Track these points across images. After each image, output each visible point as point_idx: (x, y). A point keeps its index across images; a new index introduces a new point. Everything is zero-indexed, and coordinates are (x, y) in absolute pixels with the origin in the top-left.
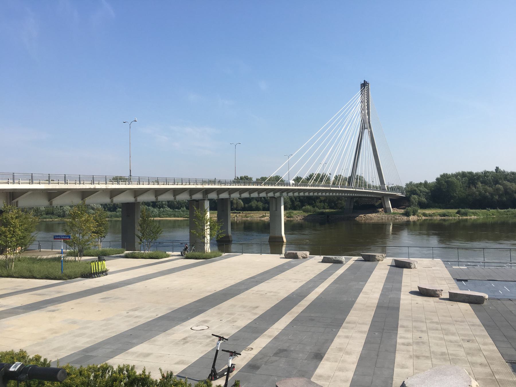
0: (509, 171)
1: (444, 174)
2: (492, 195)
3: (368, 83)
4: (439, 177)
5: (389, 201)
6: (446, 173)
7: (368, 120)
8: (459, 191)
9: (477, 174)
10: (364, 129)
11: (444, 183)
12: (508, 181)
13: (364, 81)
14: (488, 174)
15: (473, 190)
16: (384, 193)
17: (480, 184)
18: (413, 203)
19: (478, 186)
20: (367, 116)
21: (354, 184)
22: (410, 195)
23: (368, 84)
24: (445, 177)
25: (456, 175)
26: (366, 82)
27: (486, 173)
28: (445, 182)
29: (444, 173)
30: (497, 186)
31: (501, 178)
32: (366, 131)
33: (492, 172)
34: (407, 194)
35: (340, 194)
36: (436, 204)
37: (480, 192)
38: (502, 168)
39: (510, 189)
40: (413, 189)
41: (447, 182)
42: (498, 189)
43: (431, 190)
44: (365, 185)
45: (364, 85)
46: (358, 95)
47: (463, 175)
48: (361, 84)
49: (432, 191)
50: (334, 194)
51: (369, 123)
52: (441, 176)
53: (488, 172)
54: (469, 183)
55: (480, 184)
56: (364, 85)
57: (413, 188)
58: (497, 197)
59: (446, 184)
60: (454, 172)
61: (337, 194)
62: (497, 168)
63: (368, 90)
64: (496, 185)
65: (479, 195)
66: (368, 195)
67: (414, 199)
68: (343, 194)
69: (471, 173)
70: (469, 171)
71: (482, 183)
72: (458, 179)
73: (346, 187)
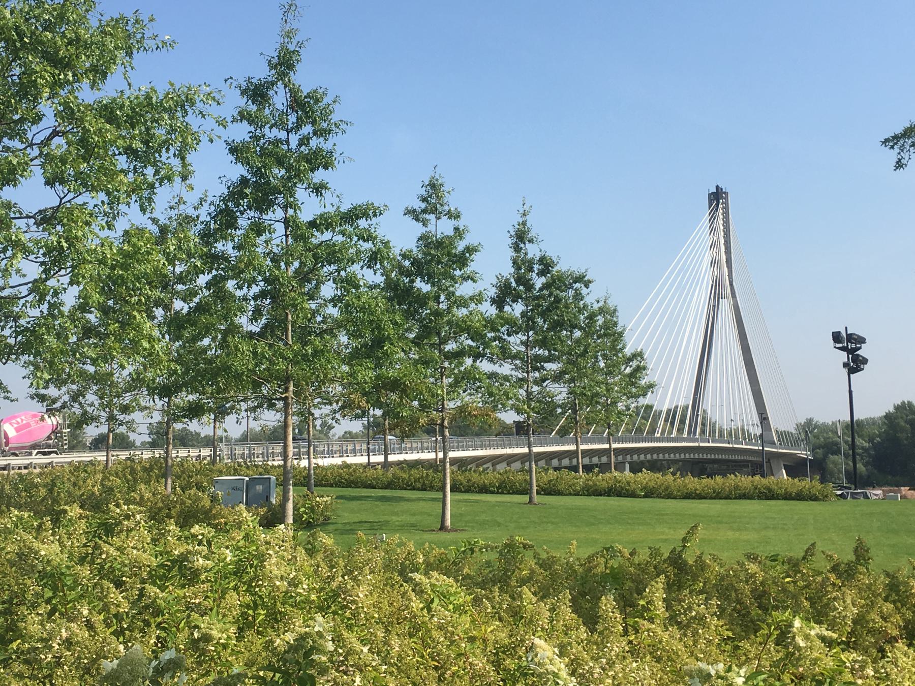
3: (725, 193)
4: (892, 410)
5: (784, 471)
6: (908, 402)
7: (727, 277)
10: (719, 298)
11: (903, 424)
13: (717, 187)
16: (776, 450)
18: (832, 475)
22: (825, 456)
26: (720, 190)
29: (904, 402)
32: (725, 306)
34: (817, 453)
35: (655, 456)
40: (830, 440)
44: (721, 435)
45: (717, 197)
46: (706, 220)
48: (710, 195)
49: (875, 447)
50: (642, 457)
52: (897, 408)
56: (717, 197)
57: (828, 438)
59: (908, 426)
61: (649, 457)
66: (692, 455)
68: (661, 456)
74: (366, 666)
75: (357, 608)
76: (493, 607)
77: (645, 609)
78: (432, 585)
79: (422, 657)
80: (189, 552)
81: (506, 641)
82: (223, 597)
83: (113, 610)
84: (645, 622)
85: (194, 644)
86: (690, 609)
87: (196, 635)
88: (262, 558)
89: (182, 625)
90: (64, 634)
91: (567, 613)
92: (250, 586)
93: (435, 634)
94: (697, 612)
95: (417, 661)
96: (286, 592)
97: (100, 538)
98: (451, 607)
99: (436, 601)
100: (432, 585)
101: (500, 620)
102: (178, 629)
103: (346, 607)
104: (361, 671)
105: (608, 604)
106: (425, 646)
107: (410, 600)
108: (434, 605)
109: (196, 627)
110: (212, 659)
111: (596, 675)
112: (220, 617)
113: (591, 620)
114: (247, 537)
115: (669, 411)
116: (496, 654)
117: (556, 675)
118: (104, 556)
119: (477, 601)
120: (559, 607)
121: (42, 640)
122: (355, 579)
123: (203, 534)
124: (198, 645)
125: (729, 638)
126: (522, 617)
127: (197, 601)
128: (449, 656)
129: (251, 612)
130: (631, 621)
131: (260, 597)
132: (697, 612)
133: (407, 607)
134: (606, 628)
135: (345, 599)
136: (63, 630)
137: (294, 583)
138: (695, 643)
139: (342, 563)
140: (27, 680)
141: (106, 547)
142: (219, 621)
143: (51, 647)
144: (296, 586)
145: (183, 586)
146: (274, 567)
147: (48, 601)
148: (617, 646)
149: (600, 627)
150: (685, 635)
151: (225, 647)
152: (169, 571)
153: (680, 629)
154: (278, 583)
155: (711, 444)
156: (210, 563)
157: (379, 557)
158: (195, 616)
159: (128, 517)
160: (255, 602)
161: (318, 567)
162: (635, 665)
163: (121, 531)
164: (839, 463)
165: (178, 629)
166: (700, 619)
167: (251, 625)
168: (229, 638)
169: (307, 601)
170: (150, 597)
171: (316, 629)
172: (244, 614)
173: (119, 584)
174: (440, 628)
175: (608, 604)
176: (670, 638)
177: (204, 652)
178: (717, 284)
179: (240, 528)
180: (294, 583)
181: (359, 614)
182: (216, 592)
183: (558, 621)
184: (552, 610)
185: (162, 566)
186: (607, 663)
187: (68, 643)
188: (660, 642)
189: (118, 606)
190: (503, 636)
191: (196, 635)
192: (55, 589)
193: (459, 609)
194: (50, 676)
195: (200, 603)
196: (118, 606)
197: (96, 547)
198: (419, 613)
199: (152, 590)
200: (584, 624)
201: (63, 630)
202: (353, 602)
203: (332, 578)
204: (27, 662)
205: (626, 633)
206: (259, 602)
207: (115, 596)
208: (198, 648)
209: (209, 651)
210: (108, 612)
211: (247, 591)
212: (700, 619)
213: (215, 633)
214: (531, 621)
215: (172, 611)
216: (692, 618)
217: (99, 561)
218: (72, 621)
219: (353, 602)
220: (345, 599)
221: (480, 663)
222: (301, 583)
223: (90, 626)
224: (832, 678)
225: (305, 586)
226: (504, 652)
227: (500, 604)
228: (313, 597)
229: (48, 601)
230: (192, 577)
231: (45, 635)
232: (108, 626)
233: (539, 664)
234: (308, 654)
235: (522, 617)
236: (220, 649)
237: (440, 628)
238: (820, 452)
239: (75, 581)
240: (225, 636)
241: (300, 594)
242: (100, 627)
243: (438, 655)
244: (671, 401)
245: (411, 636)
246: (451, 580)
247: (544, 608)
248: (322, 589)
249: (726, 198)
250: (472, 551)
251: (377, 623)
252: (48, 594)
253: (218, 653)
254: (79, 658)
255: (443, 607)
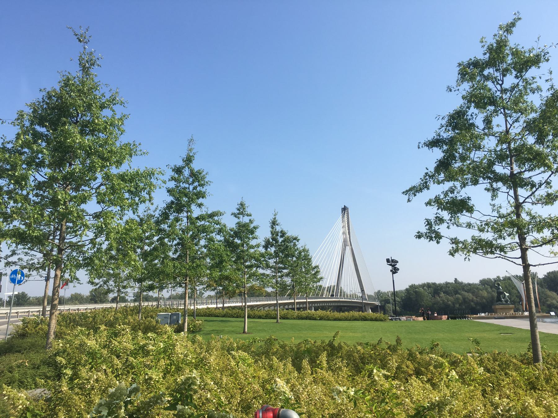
0: (466, 283)
1: (412, 285)
2: (453, 303)
4: (408, 287)
8: (426, 300)
9: (440, 284)
12: (466, 291)
14: (449, 285)
15: (437, 299)
17: (442, 294)
18: (388, 311)
19: (441, 295)
20: (348, 236)
21: (337, 295)
23: (348, 208)
24: (412, 287)
25: (423, 286)
27: (447, 284)
28: (413, 291)
30: (457, 295)
31: (460, 289)
32: (348, 249)
33: (452, 283)
35: (323, 304)
36: (408, 312)
37: (443, 301)
38: (460, 280)
39: (468, 298)
41: (416, 292)
42: (458, 299)
43: (402, 299)
45: (345, 209)
47: (428, 285)
48: (342, 209)
49: (403, 300)
51: (350, 241)
52: (410, 286)
53: (449, 283)
54: (434, 292)
55: (442, 294)
56: (345, 209)
58: (457, 306)
60: (420, 283)
61: (321, 304)
62: (456, 279)
63: (348, 214)
64: (456, 294)
65: (443, 303)
67: (389, 307)
69: (434, 284)
70: (433, 282)
71: (444, 293)
72: (425, 290)
73: (328, 298)
74: (212, 390)
75: (210, 365)
76: (262, 364)
77: (319, 364)
78: (239, 356)
79: (235, 384)
80: (147, 344)
81: (267, 378)
82: (158, 361)
83: (115, 367)
84: (319, 370)
85: (146, 381)
86: (336, 364)
87: (146, 377)
88: (174, 346)
89: (142, 372)
90: (95, 377)
91: (290, 366)
92: (169, 357)
93: (240, 375)
94: (339, 366)
95: (233, 386)
96: (183, 359)
97: (112, 338)
98: (246, 364)
99: (240, 362)
100: (239, 356)
101: (265, 369)
102: (140, 374)
103: (206, 365)
104: (210, 391)
105: (305, 363)
106: (236, 380)
107: (231, 361)
108: (239, 364)
109: (147, 374)
110: (153, 387)
111: (301, 391)
112: (157, 370)
113: (299, 368)
114: (168, 338)
115: (328, 287)
116: (263, 383)
117: (284, 392)
118: (113, 345)
119: (256, 362)
120: (287, 364)
121: (86, 379)
122: (210, 354)
123: (152, 336)
124: (147, 381)
125: (351, 375)
126: (273, 368)
127: (148, 363)
128: (245, 384)
129: (169, 367)
130: (314, 369)
131: (173, 361)
132: (339, 366)
133: (229, 364)
134: (305, 372)
135: (205, 362)
136: (95, 376)
137: (186, 356)
138: (338, 377)
139: (205, 347)
140: (80, 396)
141: (114, 342)
142: (156, 371)
143: (90, 382)
144: (187, 357)
145: (143, 357)
146: (179, 349)
147: (90, 364)
148: (309, 379)
149: (302, 372)
150: (334, 374)
151: (158, 382)
152: (138, 351)
153: (332, 372)
154: (180, 356)
155: (344, 300)
156: (154, 348)
157: (219, 345)
158: (147, 369)
159: (123, 330)
160: (171, 363)
161: (196, 349)
162: (315, 387)
163: (120, 335)
164: (390, 307)
165: (140, 374)
166: (340, 368)
167: (169, 372)
168: (160, 378)
169: (191, 362)
170: (130, 362)
171: (193, 376)
172: (166, 368)
173: (118, 357)
174: (242, 372)
175: (305, 363)
176: (328, 376)
177: (150, 384)
178: (345, 241)
179: (166, 334)
180: (186, 356)
181: (211, 368)
182: (156, 359)
183: (287, 369)
184: (285, 365)
185: (135, 349)
186: (305, 386)
187: (97, 381)
188: (325, 377)
189: (117, 365)
190: (266, 376)
191: (146, 377)
192: (93, 359)
193: (249, 365)
194: (89, 394)
195: (149, 364)
196: (117, 365)
197: (110, 342)
198: (234, 367)
199: (131, 359)
200: (297, 370)
201: (95, 376)
202: (209, 363)
203: (201, 353)
204: (80, 388)
205: (312, 374)
206: (172, 363)
207: (116, 361)
208: (147, 382)
209: (152, 383)
210: (113, 368)
211: (168, 359)
212: (340, 368)
213: (154, 376)
214: (276, 370)
215: (139, 367)
216: (337, 367)
217: (111, 347)
218: (99, 372)
219: (209, 363)
220: (205, 362)
221: (257, 387)
222: (189, 355)
223: (106, 374)
224: (388, 392)
225: (190, 357)
226: (266, 382)
227: (265, 363)
228: (193, 361)
229: (90, 364)
230: (146, 353)
231: (88, 377)
232: (113, 373)
233: (278, 388)
234: (189, 386)
235: (273, 368)
236: (156, 382)
237: (242, 372)
238: (383, 302)
239: (101, 356)
240: (158, 377)
241: (188, 360)
242: (110, 374)
243: (241, 383)
244: (329, 284)
245: (231, 376)
246: (246, 354)
247: (281, 364)
248: (197, 358)
249: (348, 210)
250: (255, 342)
251: (218, 371)
252: (90, 361)
253: (155, 385)
254: (101, 386)
255: (243, 364)
